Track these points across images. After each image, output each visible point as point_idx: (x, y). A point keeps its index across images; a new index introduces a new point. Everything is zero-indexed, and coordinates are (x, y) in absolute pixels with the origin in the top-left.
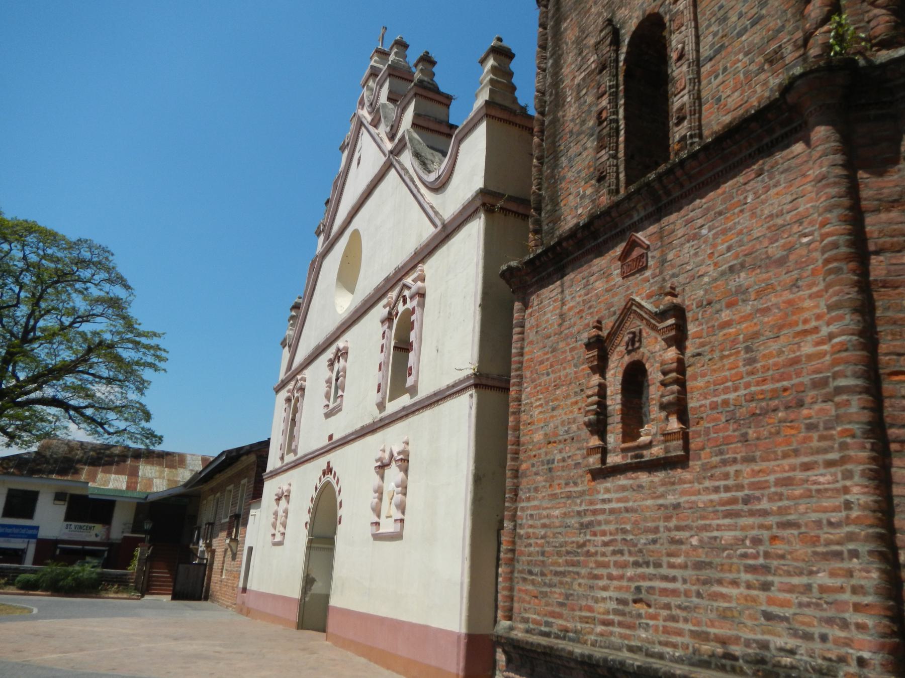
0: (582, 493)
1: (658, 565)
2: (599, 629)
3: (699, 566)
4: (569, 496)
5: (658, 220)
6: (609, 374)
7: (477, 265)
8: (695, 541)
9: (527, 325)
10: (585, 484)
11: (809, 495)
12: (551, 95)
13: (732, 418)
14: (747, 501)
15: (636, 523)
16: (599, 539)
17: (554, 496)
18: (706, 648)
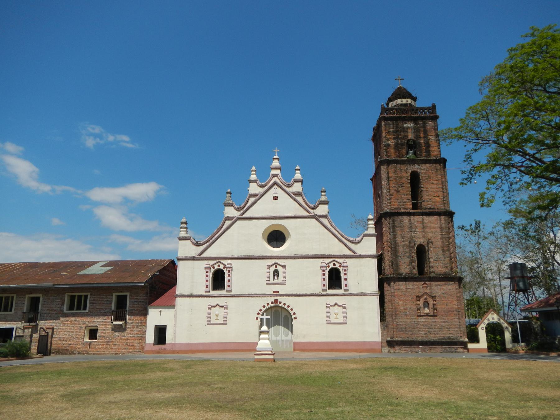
0: (415, 319)
1: (432, 328)
2: (421, 337)
3: (439, 328)
4: (412, 319)
5: (430, 282)
6: (420, 302)
7: (375, 269)
8: (439, 326)
9: (395, 287)
10: (416, 317)
11: (455, 321)
12: (393, 241)
13: (444, 312)
14: (447, 321)
15: (427, 323)
16: (420, 325)
17: (408, 318)
18: (441, 337)
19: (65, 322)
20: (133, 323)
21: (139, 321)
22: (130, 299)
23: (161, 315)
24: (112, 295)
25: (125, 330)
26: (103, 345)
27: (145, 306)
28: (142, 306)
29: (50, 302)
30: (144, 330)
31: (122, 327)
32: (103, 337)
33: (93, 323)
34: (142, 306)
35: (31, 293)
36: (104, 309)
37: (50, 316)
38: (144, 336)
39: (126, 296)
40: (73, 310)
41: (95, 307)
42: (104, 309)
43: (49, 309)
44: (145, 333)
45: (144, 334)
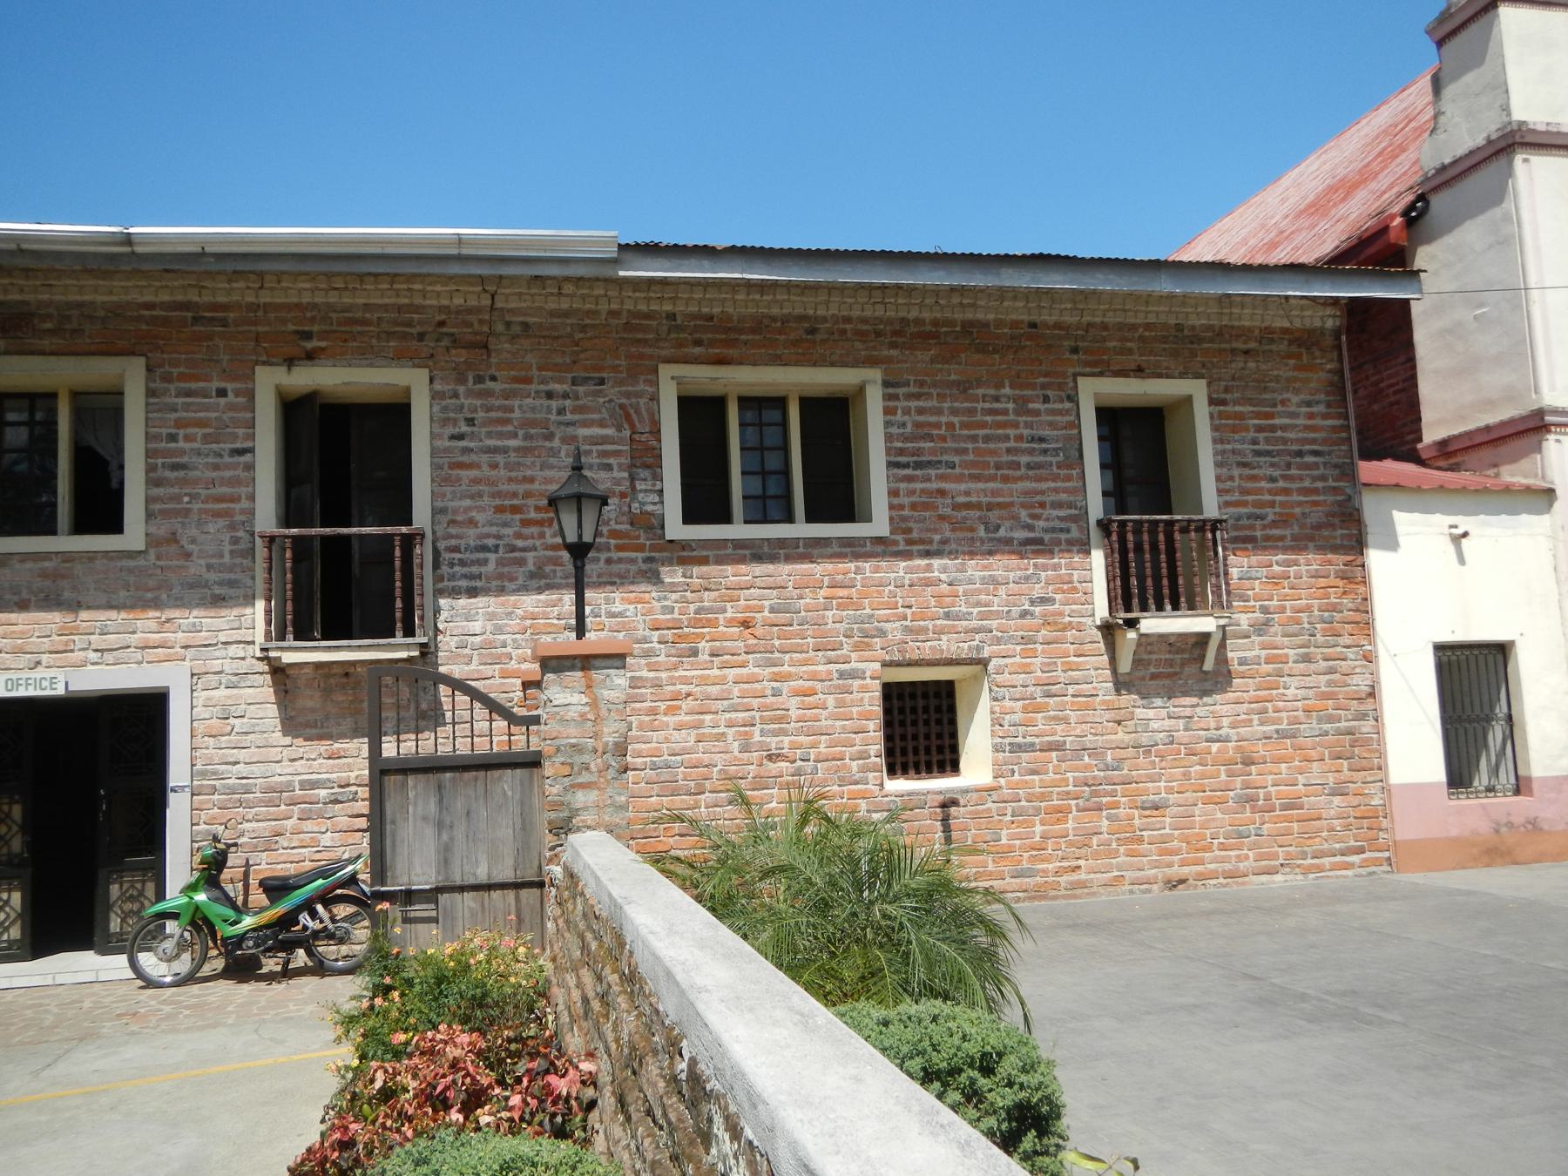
19: (695, 623)
20: (1267, 624)
21: (1309, 609)
22: (1221, 432)
23: (1462, 561)
24: (1073, 398)
25: (1219, 679)
26: (1063, 812)
27: (1335, 490)
28: (1316, 491)
29: (513, 443)
30: (1360, 683)
31: (1202, 659)
32: (1050, 747)
33: (939, 632)
34: (1316, 491)
35: (311, 356)
36: (1023, 514)
37: (532, 576)
38: (1367, 726)
39: (1188, 400)
40: (725, 518)
41: (942, 493)
42: (1023, 514)
43: (515, 509)
44: (1368, 705)
45: (1362, 716)
